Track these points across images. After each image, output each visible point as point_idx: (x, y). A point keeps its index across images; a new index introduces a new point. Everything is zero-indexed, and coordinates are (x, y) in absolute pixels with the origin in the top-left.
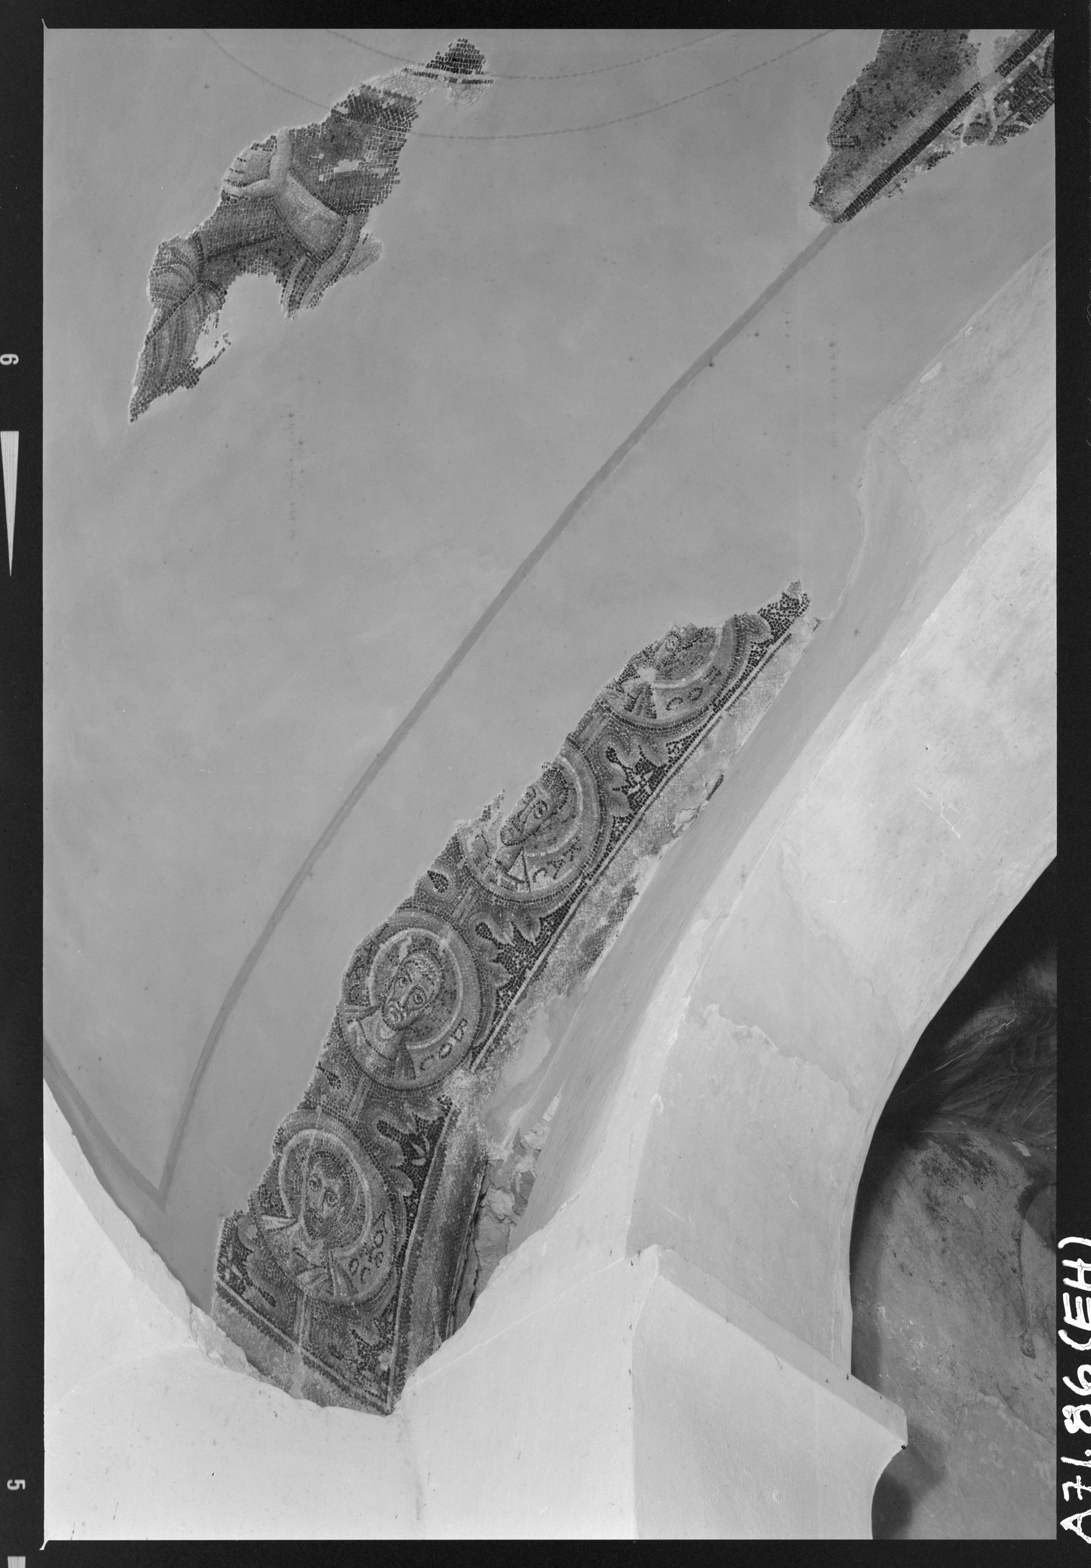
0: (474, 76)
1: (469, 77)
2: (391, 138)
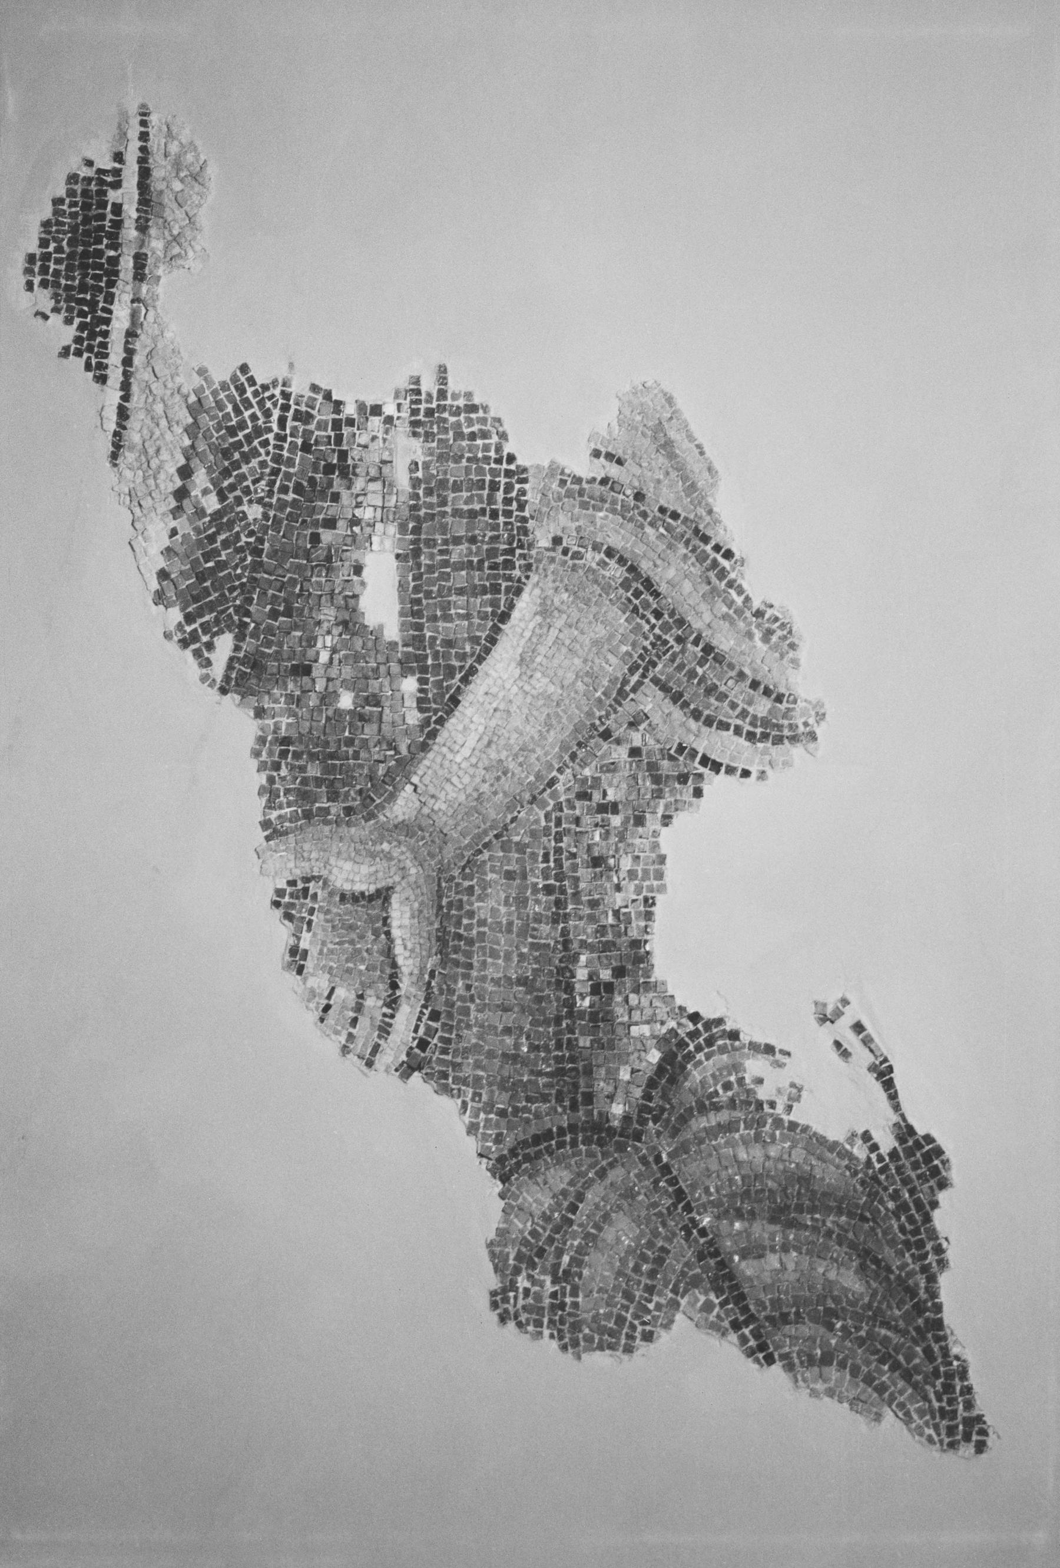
0: (127, 196)
1: (131, 211)
2: (306, 448)
